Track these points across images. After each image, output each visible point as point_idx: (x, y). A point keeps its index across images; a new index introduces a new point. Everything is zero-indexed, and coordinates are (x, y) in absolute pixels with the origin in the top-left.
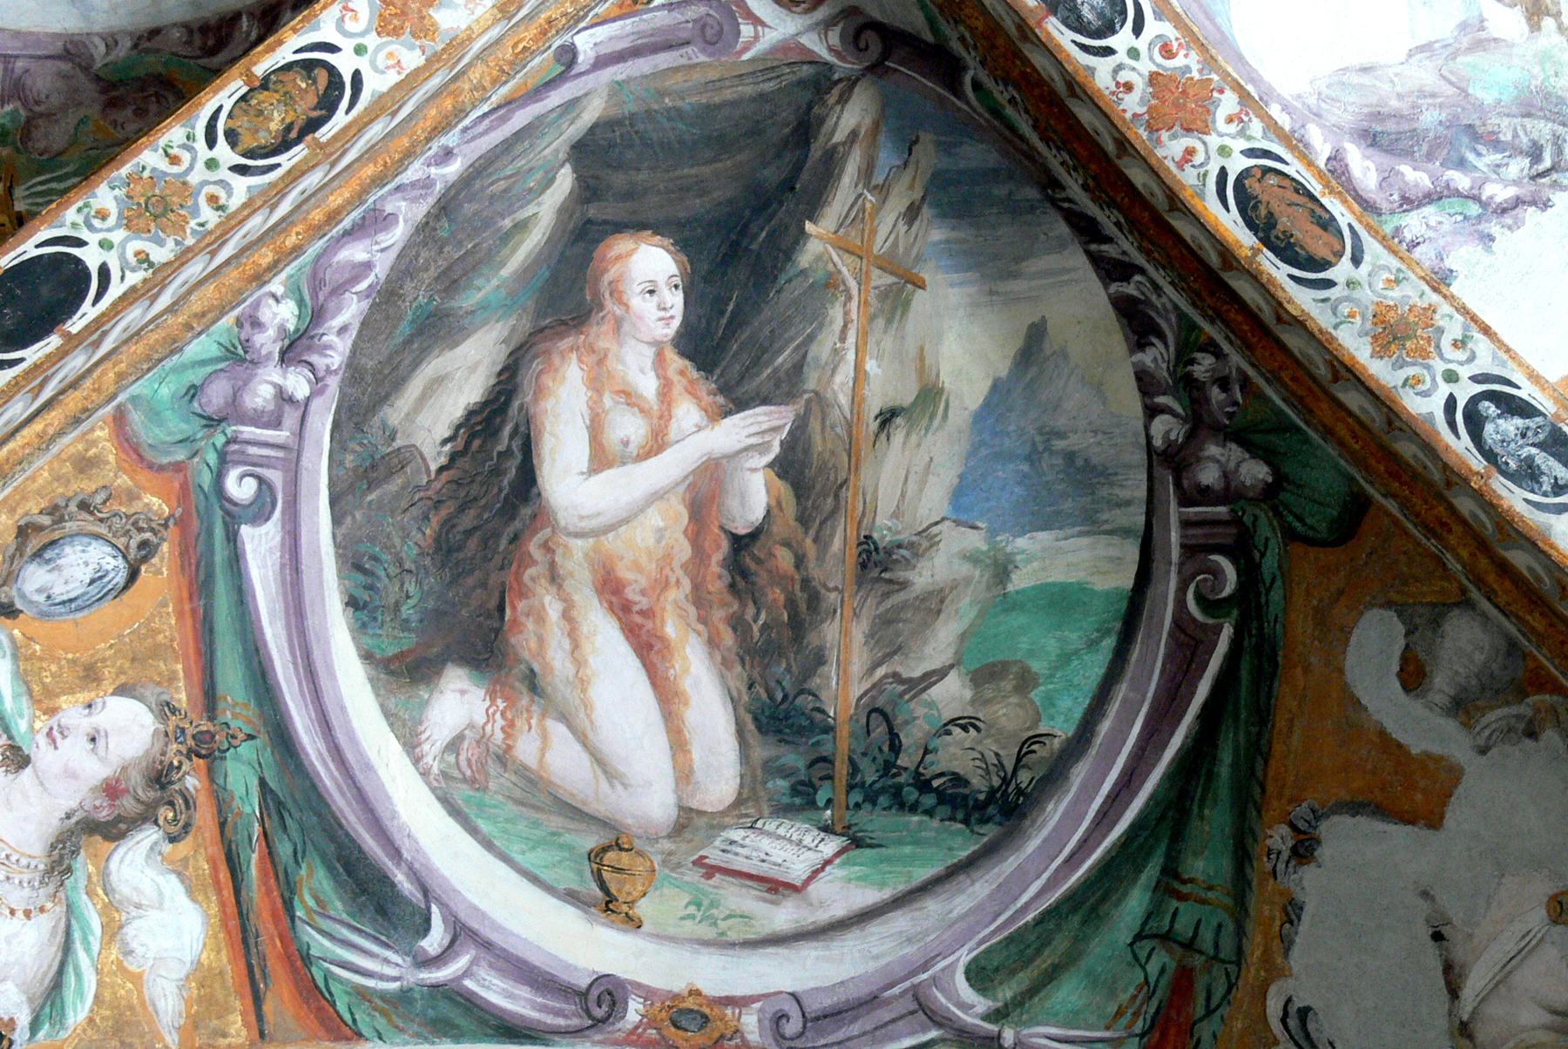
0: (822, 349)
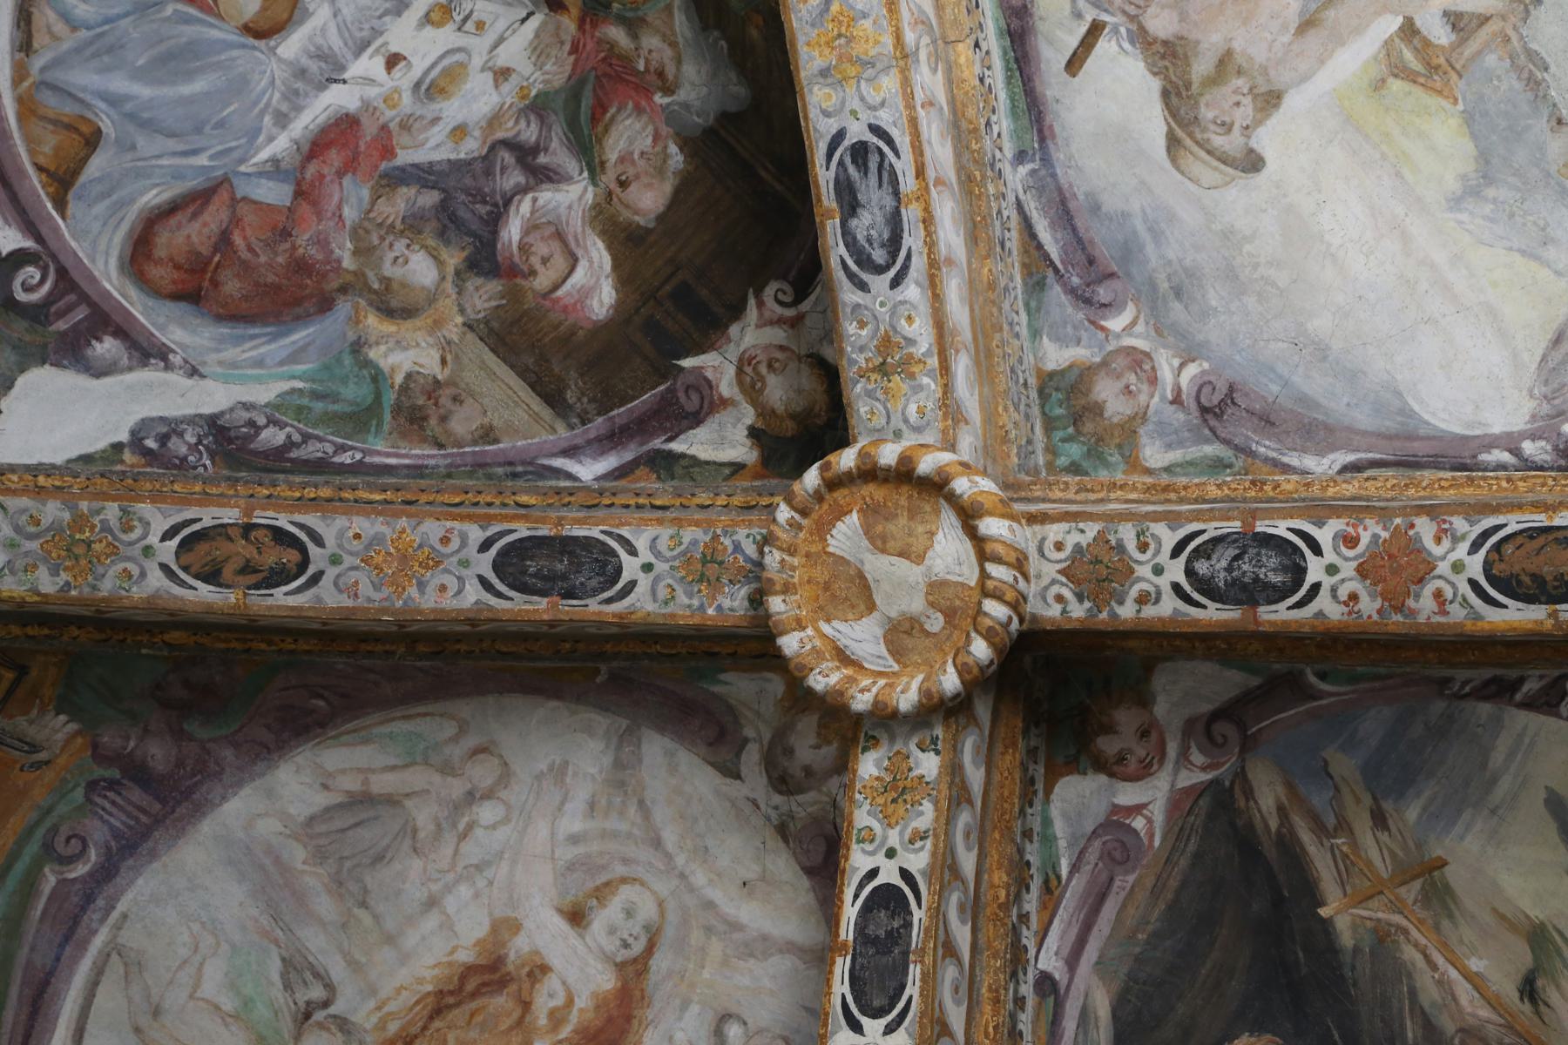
0: (1429, 993)
